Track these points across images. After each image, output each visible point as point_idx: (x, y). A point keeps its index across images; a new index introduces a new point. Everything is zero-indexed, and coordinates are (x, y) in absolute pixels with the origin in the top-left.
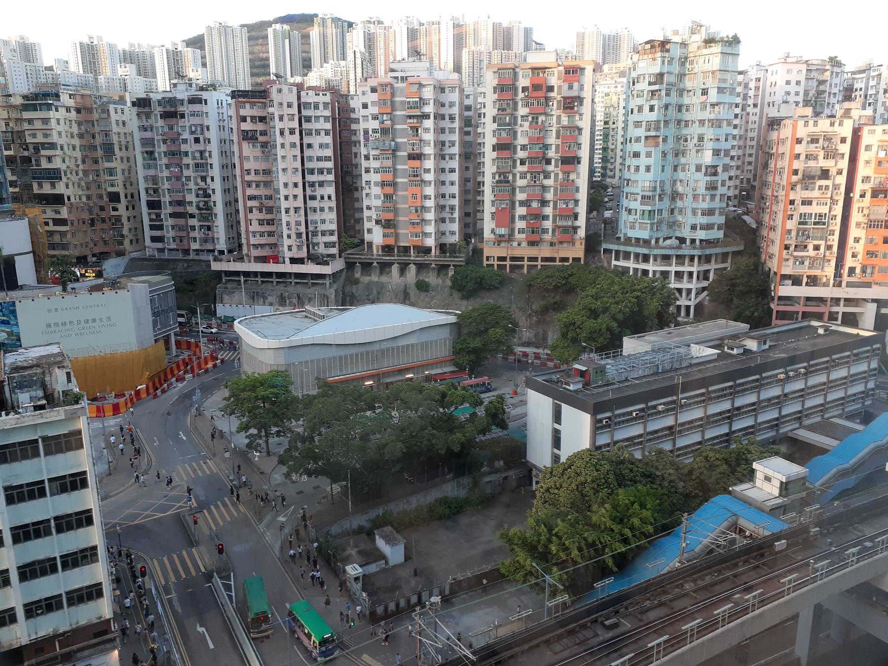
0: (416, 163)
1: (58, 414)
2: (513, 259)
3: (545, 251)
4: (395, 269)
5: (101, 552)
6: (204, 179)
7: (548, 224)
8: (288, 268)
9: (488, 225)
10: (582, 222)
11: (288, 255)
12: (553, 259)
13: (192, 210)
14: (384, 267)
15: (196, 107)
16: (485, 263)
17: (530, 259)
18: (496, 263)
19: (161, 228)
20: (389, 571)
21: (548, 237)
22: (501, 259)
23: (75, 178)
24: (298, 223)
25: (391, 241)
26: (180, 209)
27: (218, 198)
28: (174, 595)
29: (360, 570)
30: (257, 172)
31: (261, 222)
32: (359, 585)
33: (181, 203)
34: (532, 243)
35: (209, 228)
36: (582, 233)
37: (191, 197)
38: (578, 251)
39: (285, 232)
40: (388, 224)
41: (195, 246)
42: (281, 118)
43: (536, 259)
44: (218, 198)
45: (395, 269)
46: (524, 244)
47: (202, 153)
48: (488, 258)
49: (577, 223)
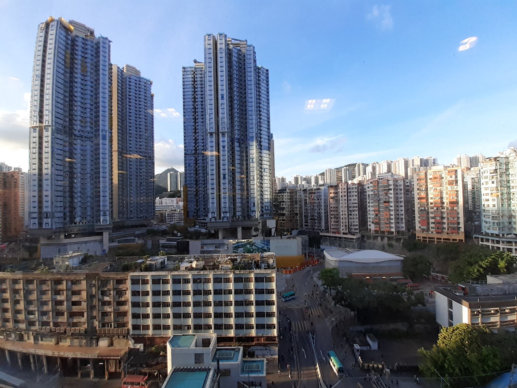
0: (387, 204)
1: (269, 271)
2: (429, 238)
3: (445, 236)
4: (379, 238)
5: (276, 314)
6: (319, 209)
7: (445, 226)
8: (342, 235)
9: (417, 225)
10: (462, 225)
11: (342, 232)
12: (449, 240)
13: (316, 218)
14: (375, 238)
15: (319, 191)
16: (417, 239)
17: (437, 239)
18: (422, 239)
19: (307, 222)
20: (370, 351)
21: (446, 231)
22: (423, 238)
23: (288, 209)
24: (346, 222)
25: (378, 229)
26: (313, 218)
27: (323, 215)
28: (297, 335)
29: (359, 347)
30: (334, 208)
31: (335, 222)
32: (358, 353)
33: (313, 216)
34: (438, 233)
35: (320, 223)
36: (462, 230)
37: (316, 215)
38: (462, 237)
39: (342, 225)
40: (377, 223)
41: (316, 228)
42: (342, 192)
43: (440, 239)
44: (323, 215)
45: (379, 238)
46: (434, 233)
47: (319, 202)
48: (418, 237)
49: (460, 226)
